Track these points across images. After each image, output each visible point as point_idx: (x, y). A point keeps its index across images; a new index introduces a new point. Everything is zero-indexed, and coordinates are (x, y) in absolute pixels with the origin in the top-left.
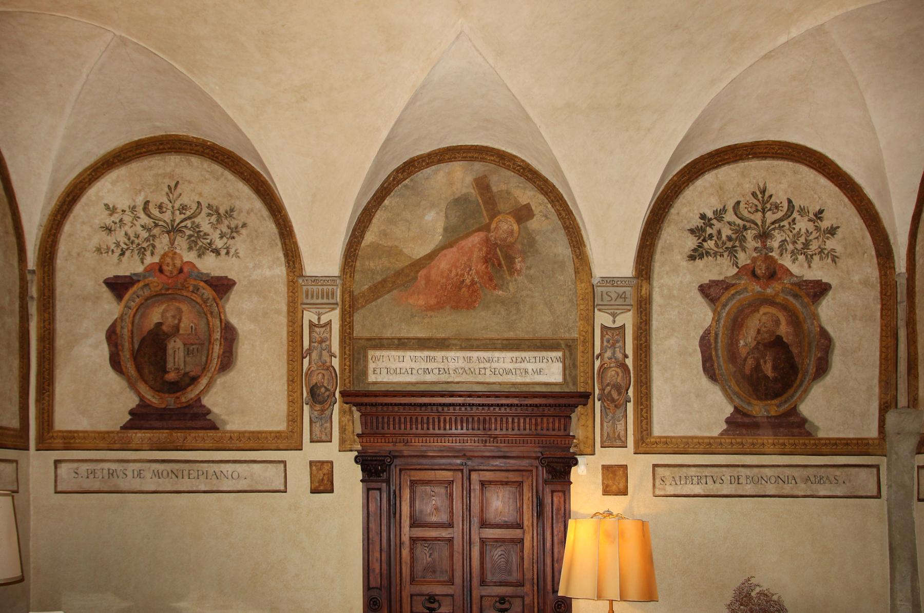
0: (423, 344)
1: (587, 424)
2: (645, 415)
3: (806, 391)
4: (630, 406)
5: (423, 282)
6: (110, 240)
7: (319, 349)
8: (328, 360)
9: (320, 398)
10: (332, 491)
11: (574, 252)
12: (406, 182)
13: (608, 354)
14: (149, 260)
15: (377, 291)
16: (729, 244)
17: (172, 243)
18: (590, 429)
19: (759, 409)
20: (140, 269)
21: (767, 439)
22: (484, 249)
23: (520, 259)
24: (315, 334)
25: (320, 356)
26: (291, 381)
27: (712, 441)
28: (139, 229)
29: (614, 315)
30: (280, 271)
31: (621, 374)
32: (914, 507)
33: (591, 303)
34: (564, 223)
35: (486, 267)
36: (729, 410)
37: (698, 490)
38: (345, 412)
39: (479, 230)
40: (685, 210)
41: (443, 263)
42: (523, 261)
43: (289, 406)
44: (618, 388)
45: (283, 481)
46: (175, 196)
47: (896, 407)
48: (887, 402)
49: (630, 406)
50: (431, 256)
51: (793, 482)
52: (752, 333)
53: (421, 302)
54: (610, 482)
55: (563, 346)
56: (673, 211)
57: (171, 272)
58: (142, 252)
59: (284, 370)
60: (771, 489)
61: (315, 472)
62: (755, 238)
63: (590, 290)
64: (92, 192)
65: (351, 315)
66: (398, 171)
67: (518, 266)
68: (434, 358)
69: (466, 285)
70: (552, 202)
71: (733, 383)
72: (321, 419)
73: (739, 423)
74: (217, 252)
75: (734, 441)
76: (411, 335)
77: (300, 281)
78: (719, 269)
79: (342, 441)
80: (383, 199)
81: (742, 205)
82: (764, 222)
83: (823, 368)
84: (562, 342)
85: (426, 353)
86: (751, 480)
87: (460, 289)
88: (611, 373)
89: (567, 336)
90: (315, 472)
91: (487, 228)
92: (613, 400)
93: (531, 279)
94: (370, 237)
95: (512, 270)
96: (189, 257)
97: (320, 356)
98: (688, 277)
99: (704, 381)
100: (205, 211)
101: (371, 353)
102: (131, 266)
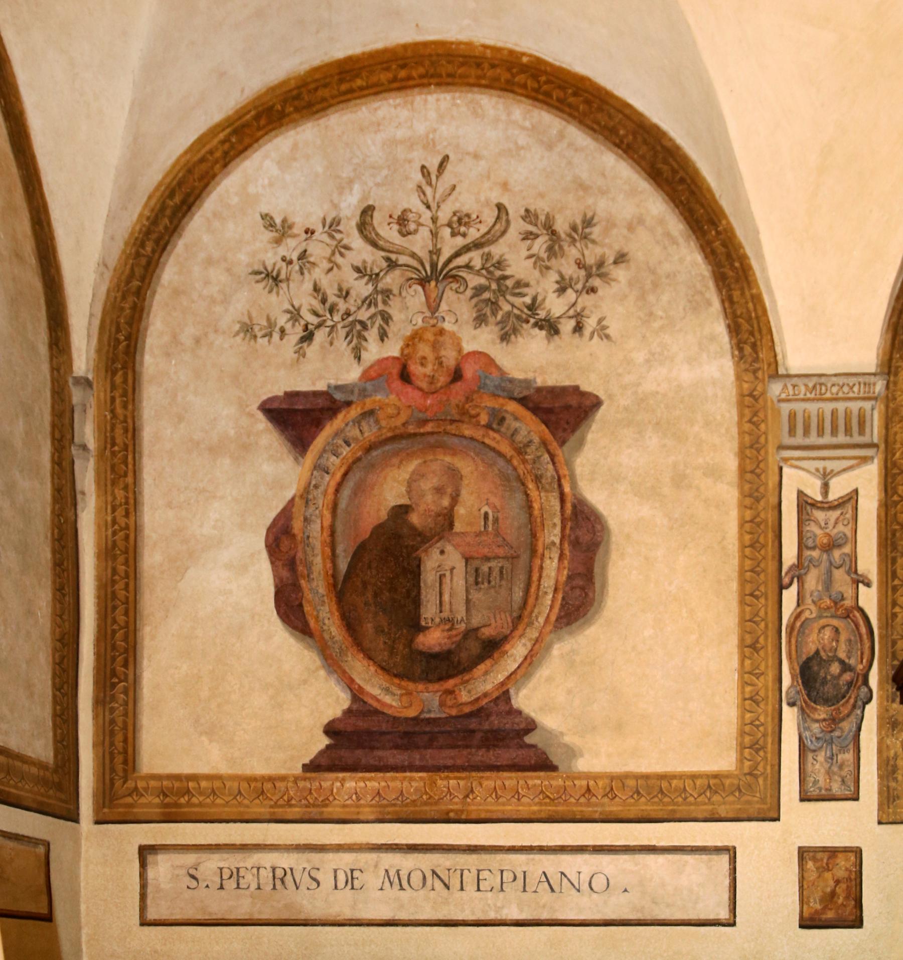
6: (276, 305)
7: (825, 565)
8: (849, 592)
9: (829, 690)
10: (857, 923)
14: (374, 351)
17: (433, 307)
20: (352, 374)
24: (813, 528)
25: (828, 582)
26: (749, 646)
28: (350, 278)
43: (743, 710)
45: (726, 896)
46: (440, 191)
57: (432, 380)
58: (357, 332)
61: (812, 875)
64: (229, 187)
72: (831, 742)
74: (551, 327)
77: (775, 389)
90: (812, 875)
96: (479, 340)
97: (828, 582)
100: (518, 226)
102: (329, 368)
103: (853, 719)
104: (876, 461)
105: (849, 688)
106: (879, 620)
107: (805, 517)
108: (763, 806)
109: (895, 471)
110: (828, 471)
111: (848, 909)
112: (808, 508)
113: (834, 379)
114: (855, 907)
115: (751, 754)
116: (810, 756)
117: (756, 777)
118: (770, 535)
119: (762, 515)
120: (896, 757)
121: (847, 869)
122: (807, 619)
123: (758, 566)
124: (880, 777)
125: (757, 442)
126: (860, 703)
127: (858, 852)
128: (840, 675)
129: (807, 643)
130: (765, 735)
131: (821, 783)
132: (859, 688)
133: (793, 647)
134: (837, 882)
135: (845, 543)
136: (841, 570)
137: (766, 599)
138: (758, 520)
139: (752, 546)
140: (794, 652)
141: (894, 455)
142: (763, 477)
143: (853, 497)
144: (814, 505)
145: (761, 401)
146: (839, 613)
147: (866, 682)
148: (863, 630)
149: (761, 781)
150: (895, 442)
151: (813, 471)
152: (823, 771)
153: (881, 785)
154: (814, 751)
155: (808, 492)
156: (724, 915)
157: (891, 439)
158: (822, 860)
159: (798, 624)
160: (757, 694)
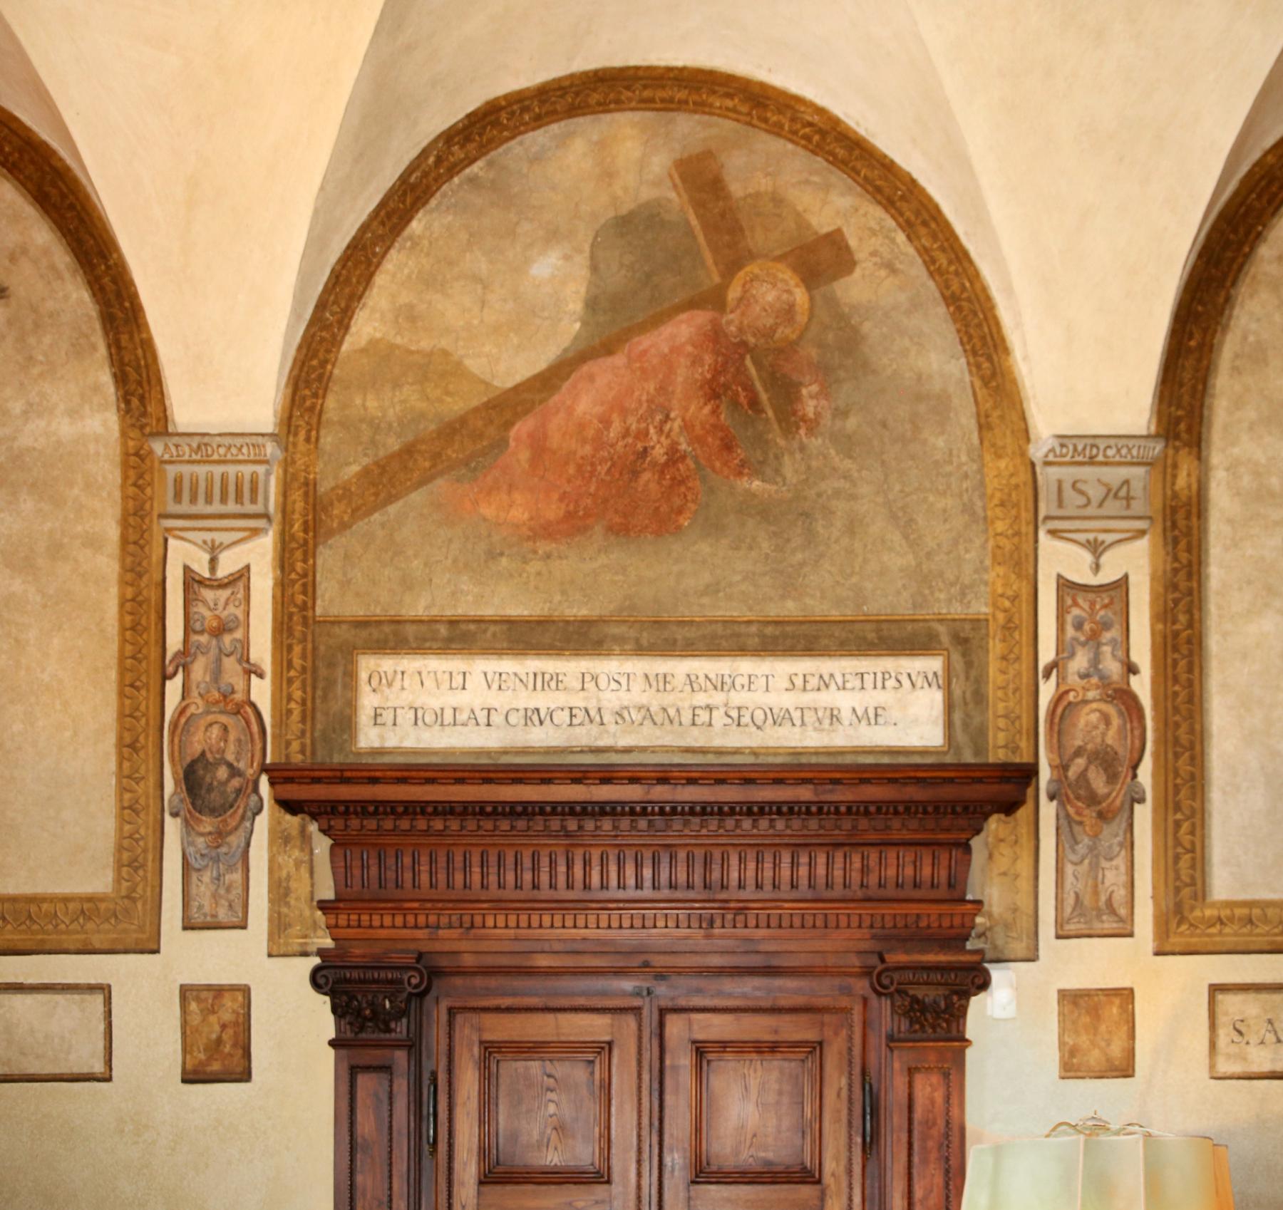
0: (522, 637)
1: (1020, 870)
4: (1144, 816)
5: (524, 455)
7: (214, 652)
8: (240, 685)
10: (245, 1076)
11: (974, 367)
12: (476, 168)
13: (1080, 662)
15: (387, 479)
18: (1024, 884)
22: (708, 359)
23: (814, 388)
24: (201, 609)
25: (217, 672)
26: (128, 747)
30: (102, 423)
31: (1116, 721)
33: (1026, 516)
34: (944, 287)
35: (714, 412)
38: (287, 840)
39: (691, 305)
41: (585, 400)
42: (824, 393)
43: (122, 820)
44: (1106, 760)
45: (100, 1044)
49: (1144, 816)
50: (548, 381)
53: (519, 514)
54: (1084, 1041)
55: (945, 640)
59: (108, 716)
61: (195, 1019)
63: (1024, 476)
65: (309, 552)
66: (451, 137)
67: (810, 407)
68: (556, 678)
69: (654, 464)
70: (909, 228)
72: (217, 860)
76: (488, 611)
77: (158, 447)
79: (278, 925)
80: (406, 218)
84: (941, 629)
85: (533, 664)
87: (635, 474)
88: (1087, 717)
89: (957, 610)
90: (195, 1019)
91: (715, 300)
92: (1093, 799)
93: (847, 443)
94: (367, 326)
95: (790, 419)
97: (217, 672)
101: (367, 665)
103: (241, 833)
104: (271, 533)
105: (237, 796)
106: (273, 716)
107: (191, 596)
108: (141, 936)
109: (294, 545)
110: (217, 543)
111: (236, 1059)
112: (196, 586)
113: (218, 439)
114: (243, 1056)
115: (129, 873)
116: (194, 876)
117: (134, 900)
118: (153, 617)
119: (145, 593)
120: (289, 877)
121: (234, 1011)
122: (192, 715)
123: (140, 652)
124: (271, 901)
125: (142, 508)
126: (249, 814)
127: (246, 991)
128: (228, 780)
129: (191, 743)
130: (145, 851)
131: (207, 909)
132: (249, 796)
133: (176, 748)
134: (224, 1027)
135: (237, 627)
136: (232, 659)
137: (148, 691)
138: (140, 598)
139: (133, 629)
140: (176, 754)
141: (292, 526)
142: (147, 549)
143: (242, 576)
144: (202, 582)
145: (148, 462)
146: (229, 708)
147: (256, 789)
148: (255, 728)
149: (139, 905)
150: (293, 513)
151: (200, 542)
152: (208, 893)
153: (271, 910)
154: (199, 870)
155: (195, 567)
156: (99, 1068)
157: (289, 508)
158: (206, 1000)
159: (183, 720)
160: (137, 802)
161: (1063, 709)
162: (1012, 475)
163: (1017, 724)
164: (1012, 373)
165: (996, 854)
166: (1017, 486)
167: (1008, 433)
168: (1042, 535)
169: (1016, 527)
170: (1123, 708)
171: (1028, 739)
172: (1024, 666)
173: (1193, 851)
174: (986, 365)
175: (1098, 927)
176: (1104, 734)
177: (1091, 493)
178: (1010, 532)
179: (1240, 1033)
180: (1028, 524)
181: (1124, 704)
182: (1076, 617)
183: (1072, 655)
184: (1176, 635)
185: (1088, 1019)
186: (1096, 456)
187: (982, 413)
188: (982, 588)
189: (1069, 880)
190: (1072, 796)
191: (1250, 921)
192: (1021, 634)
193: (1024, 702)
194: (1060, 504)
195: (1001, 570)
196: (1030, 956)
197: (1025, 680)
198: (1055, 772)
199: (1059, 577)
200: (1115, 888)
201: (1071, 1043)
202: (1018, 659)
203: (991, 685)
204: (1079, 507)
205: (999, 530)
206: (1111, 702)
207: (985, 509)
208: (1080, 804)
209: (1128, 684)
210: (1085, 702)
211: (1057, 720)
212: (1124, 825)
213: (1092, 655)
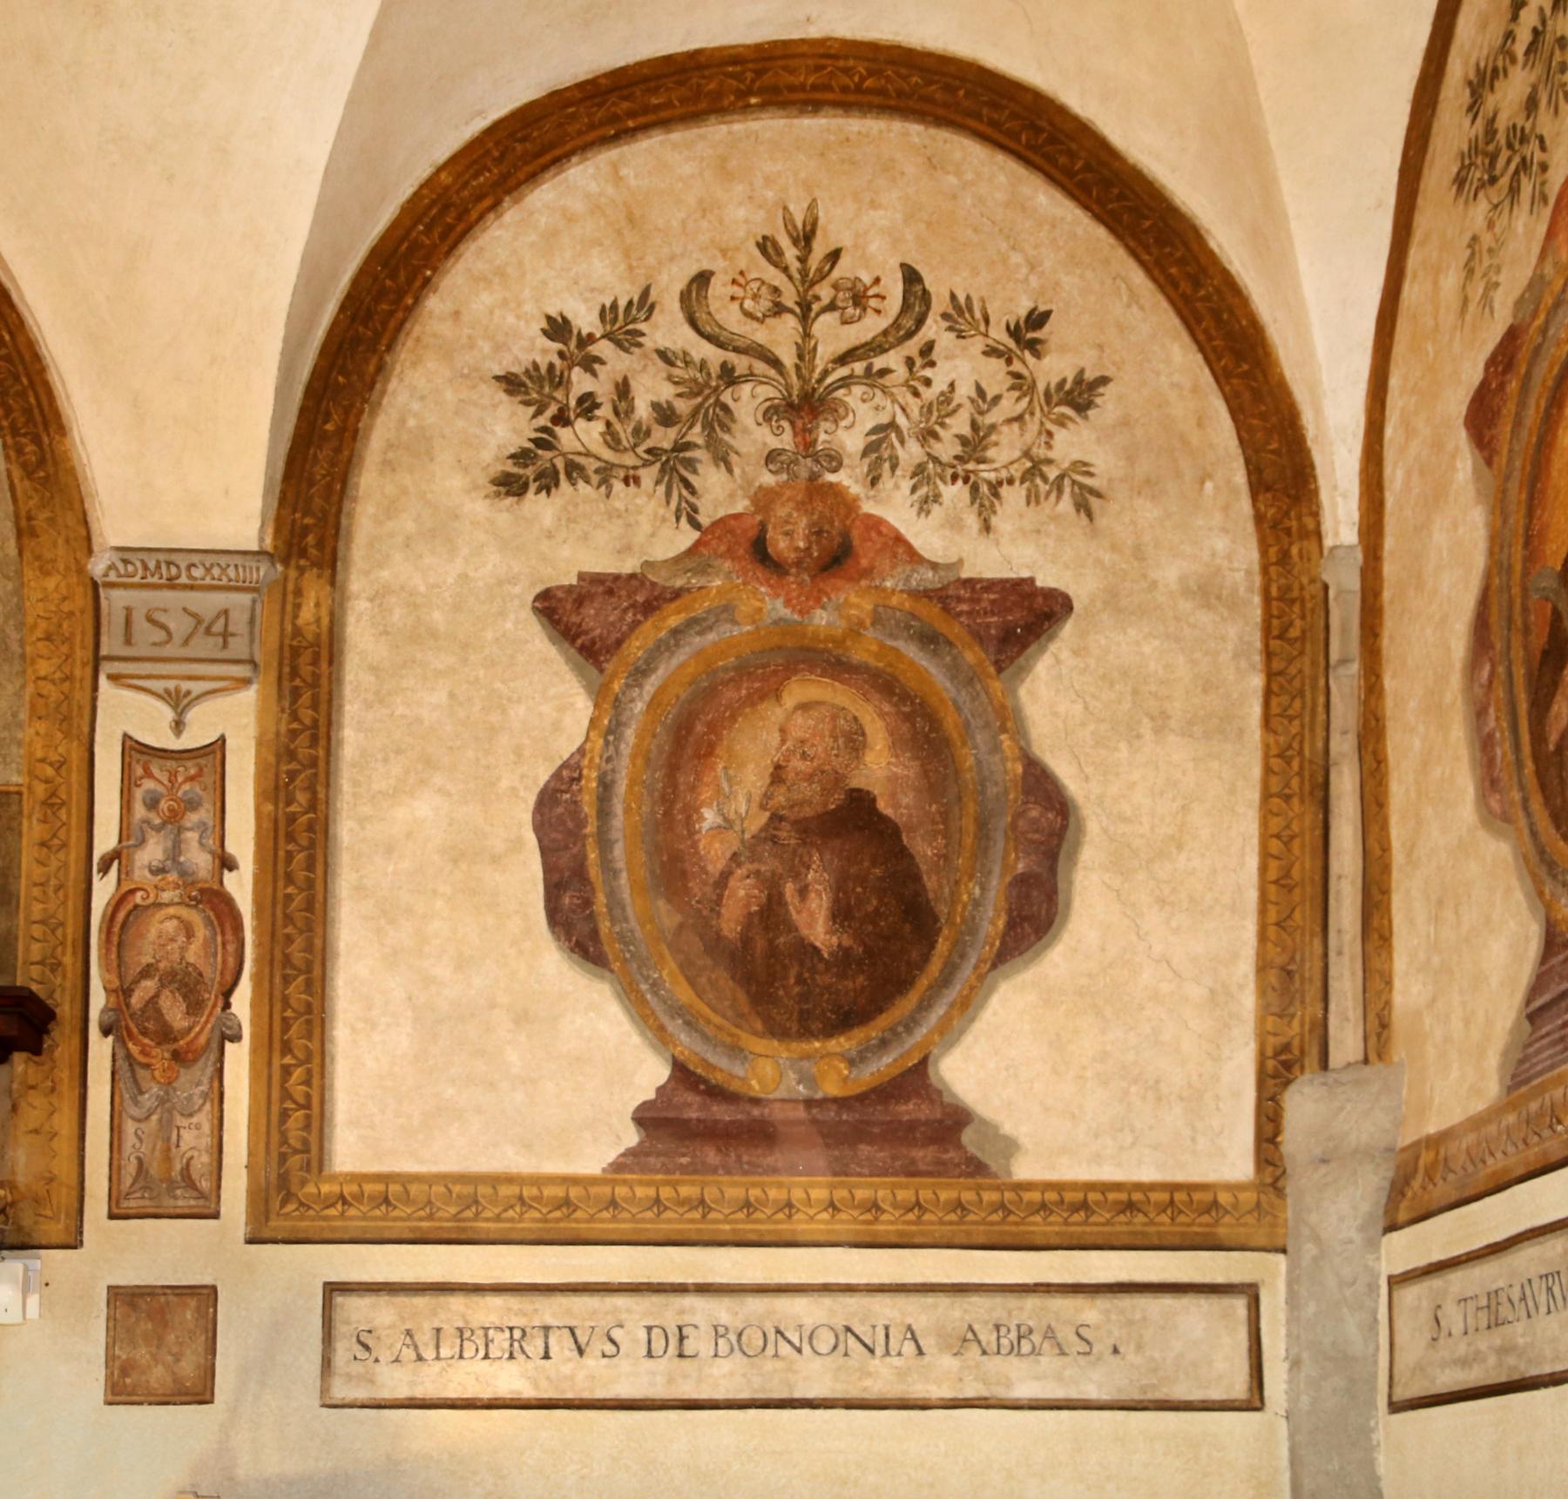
2: (299, 1091)
3: (968, 1006)
4: (238, 1058)
13: (153, 852)
16: (664, 438)
18: (64, 1145)
19: (775, 1072)
21: (806, 1185)
27: (574, 1192)
29: (180, 703)
31: (201, 932)
32: (1379, 1436)
33: (82, 654)
36: (649, 1074)
37: (509, 1379)
40: (484, 300)
44: (188, 985)
47: (1324, 1064)
48: (1286, 1048)
49: (238, 1058)
51: (909, 1348)
52: (753, 779)
54: (142, 1354)
56: (434, 304)
60: (815, 1378)
62: (770, 414)
63: (81, 600)
71: (668, 971)
73: (693, 1125)
75: (666, 1193)
78: (619, 531)
81: (719, 289)
82: (805, 353)
83: (1034, 916)
86: (734, 1340)
92: (166, 1035)
98: (493, 563)
99: (552, 962)
161: (127, 915)
162: (64, 599)
163: (59, 932)
164: (69, 459)
165: (23, 1105)
166: (71, 614)
167: (60, 542)
168: (103, 681)
169: (67, 670)
170: (211, 914)
171: (74, 953)
172: (73, 856)
173: (308, 1106)
174: (30, 448)
175: (168, 1204)
176: (183, 949)
177: (172, 626)
178: (58, 675)
179: (367, 1347)
180: (84, 665)
181: (213, 909)
182: (148, 792)
183: (142, 842)
184: (292, 819)
185: (150, 1326)
186: (178, 577)
187: (23, 514)
188: (14, 749)
189: (130, 1140)
190: (135, 1030)
191: (386, 1201)
192: (69, 814)
193: (70, 903)
194: (128, 641)
195: (42, 727)
196: (71, 1241)
197: (72, 875)
198: (113, 999)
199: (126, 737)
200: (196, 1154)
201: (124, 1357)
202: (64, 845)
203: (23, 880)
204: (155, 644)
205: (42, 673)
206: (195, 907)
207: (22, 643)
208: (146, 1041)
209: (221, 883)
210: (159, 905)
211: (116, 929)
212: (210, 1070)
213: (170, 844)
